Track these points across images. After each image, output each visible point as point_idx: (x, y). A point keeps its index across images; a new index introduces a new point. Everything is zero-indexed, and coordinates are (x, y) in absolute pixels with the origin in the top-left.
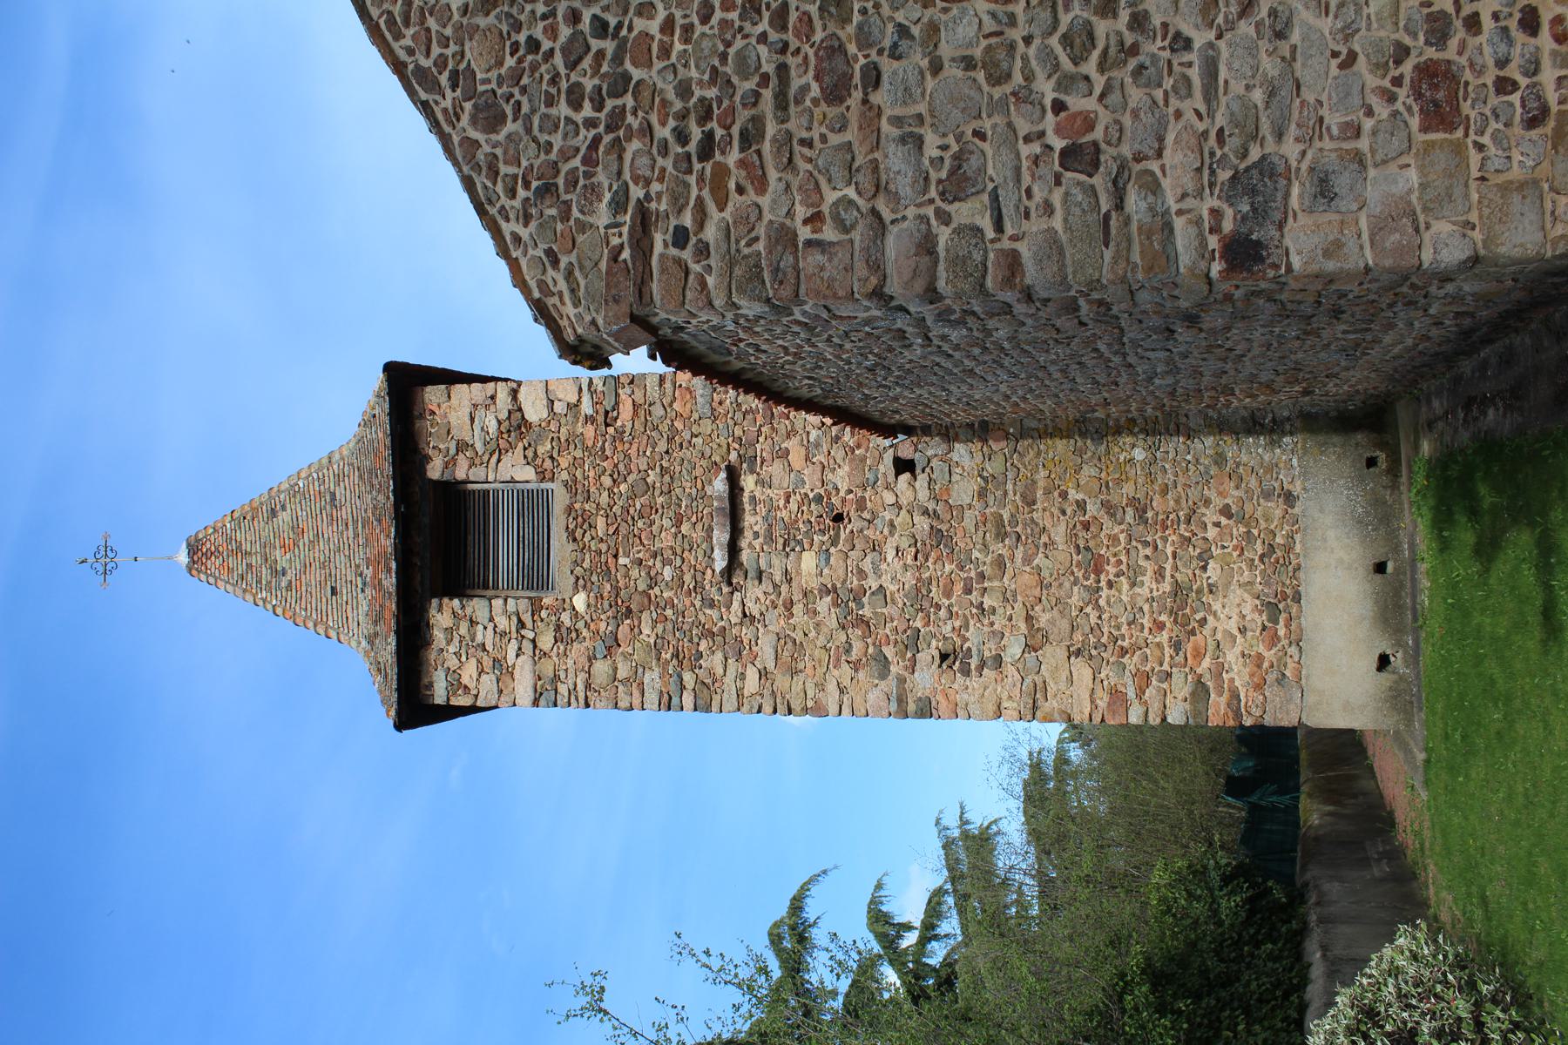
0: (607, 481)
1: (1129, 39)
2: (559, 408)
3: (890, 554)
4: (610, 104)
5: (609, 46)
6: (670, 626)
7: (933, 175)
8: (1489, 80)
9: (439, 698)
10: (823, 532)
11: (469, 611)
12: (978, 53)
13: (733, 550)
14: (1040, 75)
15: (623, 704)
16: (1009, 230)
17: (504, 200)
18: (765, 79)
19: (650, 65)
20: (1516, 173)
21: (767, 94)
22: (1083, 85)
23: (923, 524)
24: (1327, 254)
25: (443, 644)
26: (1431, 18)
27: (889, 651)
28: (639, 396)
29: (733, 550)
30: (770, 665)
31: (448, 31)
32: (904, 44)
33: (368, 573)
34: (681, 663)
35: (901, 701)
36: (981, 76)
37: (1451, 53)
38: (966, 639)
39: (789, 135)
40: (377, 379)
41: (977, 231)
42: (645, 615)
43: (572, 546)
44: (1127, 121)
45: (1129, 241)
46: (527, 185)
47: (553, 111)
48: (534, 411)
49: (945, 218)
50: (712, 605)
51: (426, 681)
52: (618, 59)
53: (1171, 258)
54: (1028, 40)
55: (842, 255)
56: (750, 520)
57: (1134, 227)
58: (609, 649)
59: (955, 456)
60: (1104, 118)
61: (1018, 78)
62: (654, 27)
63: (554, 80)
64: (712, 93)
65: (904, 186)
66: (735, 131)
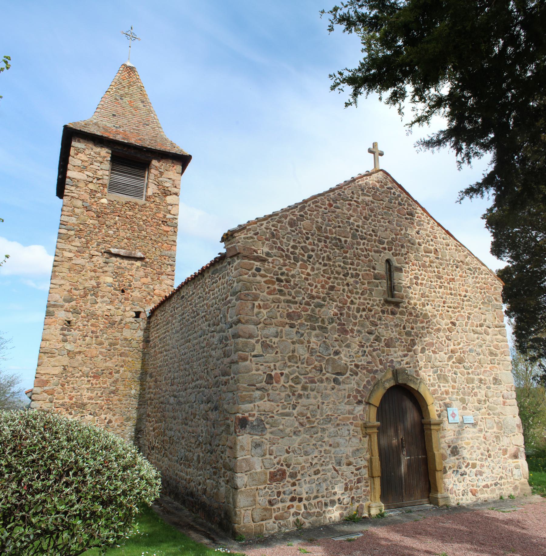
0: (144, 218)
1: (296, 393)
2: (170, 207)
3: (109, 307)
4: (292, 256)
5: (305, 258)
6: (92, 230)
7: (268, 340)
8: (281, 490)
9: (74, 143)
10: (119, 285)
11: (106, 162)
12: (296, 354)
13: (117, 255)
14: (290, 370)
15: (65, 208)
16: (253, 359)
17: (271, 223)
18: (294, 298)
19: (300, 268)
20: (258, 498)
21: (290, 298)
22: (286, 381)
23: (118, 319)
24: (241, 446)
25: (94, 150)
26: (296, 474)
27: (74, 303)
28: (170, 233)
29: (117, 255)
30: (73, 262)
31: (313, 217)
32: (299, 335)
33: (121, 130)
34: (78, 231)
35: (54, 306)
36: (290, 354)
37: (288, 479)
38: (75, 330)
39: (280, 302)
40: (188, 153)
41: (253, 350)
42: (97, 222)
43: (124, 202)
44: (277, 392)
45: (249, 391)
46: (275, 230)
47: (292, 241)
48: (170, 199)
49: (257, 342)
50: (98, 245)
51: (81, 140)
52: (302, 260)
53: (243, 403)
54: (298, 367)
55: (250, 313)
56: (125, 263)
57: (252, 393)
58: (86, 207)
59: (139, 331)
60: (279, 386)
61: (289, 364)
62: (309, 270)
63: (299, 242)
64: (292, 283)
65: (266, 332)
66: (283, 288)
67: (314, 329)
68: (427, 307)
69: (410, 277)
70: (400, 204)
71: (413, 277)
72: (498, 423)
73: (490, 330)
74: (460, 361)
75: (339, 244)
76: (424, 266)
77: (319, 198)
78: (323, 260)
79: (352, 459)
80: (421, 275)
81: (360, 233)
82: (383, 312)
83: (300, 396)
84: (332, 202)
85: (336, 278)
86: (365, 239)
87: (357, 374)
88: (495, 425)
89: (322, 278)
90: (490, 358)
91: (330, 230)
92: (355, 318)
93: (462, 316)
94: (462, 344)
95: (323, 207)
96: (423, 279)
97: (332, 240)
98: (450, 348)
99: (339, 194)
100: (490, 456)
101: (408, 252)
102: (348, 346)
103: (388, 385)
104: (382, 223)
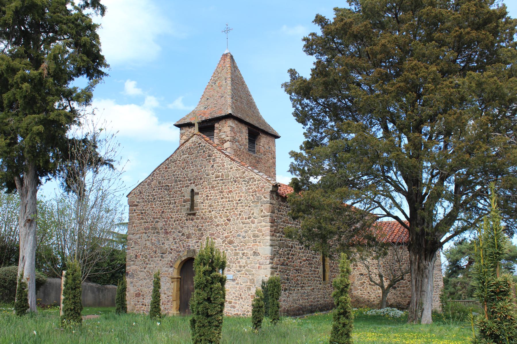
62: (154, 206)
67: (154, 233)
68: (212, 213)
70: (204, 152)
72: (250, 280)
73: (256, 220)
74: (231, 242)
75: (168, 188)
76: (213, 187)
79: (166, 292)
82: (187, 220)
83: (147, 264)
85: (165, 207)
87: (171, 253)
88: (249, 281)
89: (159, 208)
90: (253, 238)
92: (173, 225)
93: (235, 214)
94: (233, 232)
96: (211, 196)
98: (224, 235)
99: (171, 160)
100: (242, 298)
102: (168, 240)
103: (183, 259)
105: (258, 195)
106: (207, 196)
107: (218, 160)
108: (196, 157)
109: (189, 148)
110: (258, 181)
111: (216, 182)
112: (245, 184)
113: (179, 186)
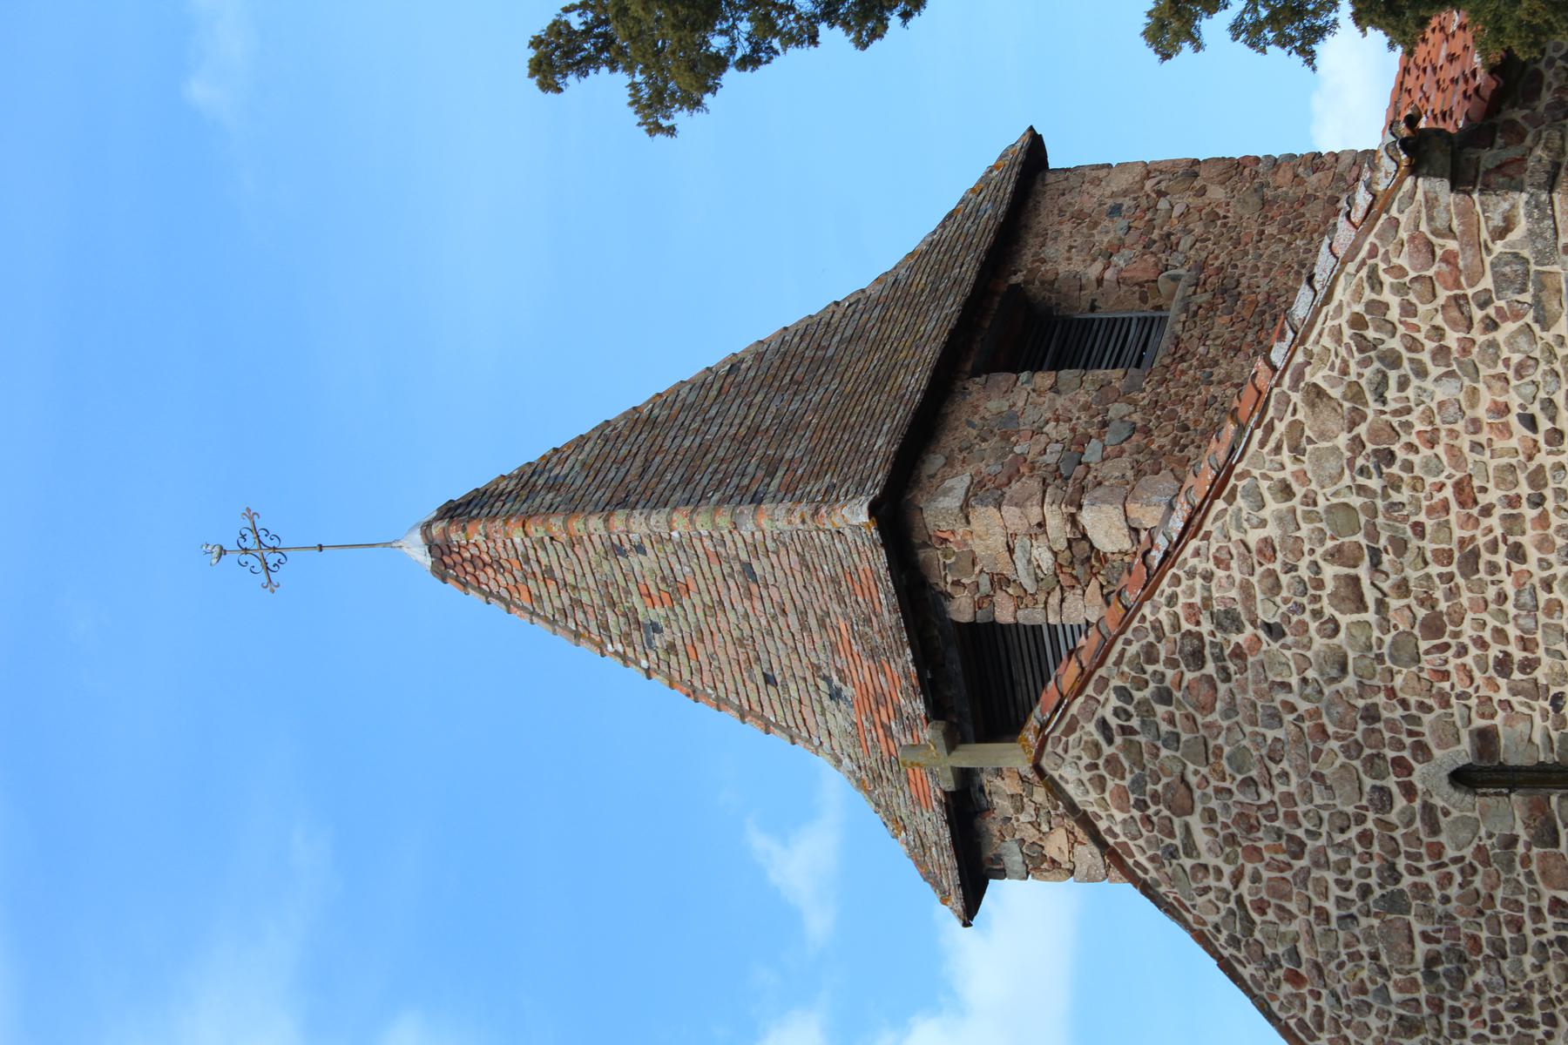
69: (1504, 694)
70: (1165, 697)
71: (1502, 682)
75: (1451, 965)
76: (1433, 627)
77: (1283, 1015)
78: (1532, 1024)
80: (1482, 644)
81: (1373, 880)
84: (1280, 973)
86: (1392, 867)
91: (1401, 990)
95: (1310, 1002)
96: (1500, 635)
97: (1441, 989)
99: (1234, 941)
101: (1391, 693)
104: (1293, 787)
105: (1487, 282)
106: (1503, 665)
107: (1225, 593)
108: (1206, 753)
109: (1141, 805)
110: (1375, 282)
111: (1394, 603)
112: (1403, 384)
113: (1430, 878)
